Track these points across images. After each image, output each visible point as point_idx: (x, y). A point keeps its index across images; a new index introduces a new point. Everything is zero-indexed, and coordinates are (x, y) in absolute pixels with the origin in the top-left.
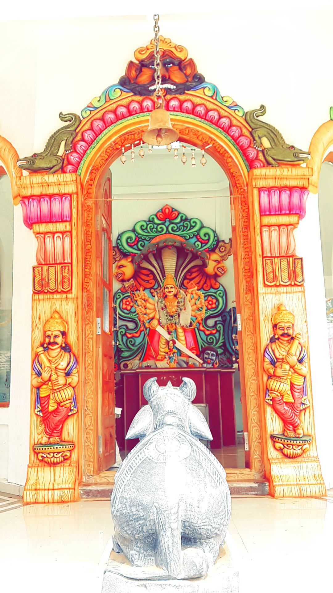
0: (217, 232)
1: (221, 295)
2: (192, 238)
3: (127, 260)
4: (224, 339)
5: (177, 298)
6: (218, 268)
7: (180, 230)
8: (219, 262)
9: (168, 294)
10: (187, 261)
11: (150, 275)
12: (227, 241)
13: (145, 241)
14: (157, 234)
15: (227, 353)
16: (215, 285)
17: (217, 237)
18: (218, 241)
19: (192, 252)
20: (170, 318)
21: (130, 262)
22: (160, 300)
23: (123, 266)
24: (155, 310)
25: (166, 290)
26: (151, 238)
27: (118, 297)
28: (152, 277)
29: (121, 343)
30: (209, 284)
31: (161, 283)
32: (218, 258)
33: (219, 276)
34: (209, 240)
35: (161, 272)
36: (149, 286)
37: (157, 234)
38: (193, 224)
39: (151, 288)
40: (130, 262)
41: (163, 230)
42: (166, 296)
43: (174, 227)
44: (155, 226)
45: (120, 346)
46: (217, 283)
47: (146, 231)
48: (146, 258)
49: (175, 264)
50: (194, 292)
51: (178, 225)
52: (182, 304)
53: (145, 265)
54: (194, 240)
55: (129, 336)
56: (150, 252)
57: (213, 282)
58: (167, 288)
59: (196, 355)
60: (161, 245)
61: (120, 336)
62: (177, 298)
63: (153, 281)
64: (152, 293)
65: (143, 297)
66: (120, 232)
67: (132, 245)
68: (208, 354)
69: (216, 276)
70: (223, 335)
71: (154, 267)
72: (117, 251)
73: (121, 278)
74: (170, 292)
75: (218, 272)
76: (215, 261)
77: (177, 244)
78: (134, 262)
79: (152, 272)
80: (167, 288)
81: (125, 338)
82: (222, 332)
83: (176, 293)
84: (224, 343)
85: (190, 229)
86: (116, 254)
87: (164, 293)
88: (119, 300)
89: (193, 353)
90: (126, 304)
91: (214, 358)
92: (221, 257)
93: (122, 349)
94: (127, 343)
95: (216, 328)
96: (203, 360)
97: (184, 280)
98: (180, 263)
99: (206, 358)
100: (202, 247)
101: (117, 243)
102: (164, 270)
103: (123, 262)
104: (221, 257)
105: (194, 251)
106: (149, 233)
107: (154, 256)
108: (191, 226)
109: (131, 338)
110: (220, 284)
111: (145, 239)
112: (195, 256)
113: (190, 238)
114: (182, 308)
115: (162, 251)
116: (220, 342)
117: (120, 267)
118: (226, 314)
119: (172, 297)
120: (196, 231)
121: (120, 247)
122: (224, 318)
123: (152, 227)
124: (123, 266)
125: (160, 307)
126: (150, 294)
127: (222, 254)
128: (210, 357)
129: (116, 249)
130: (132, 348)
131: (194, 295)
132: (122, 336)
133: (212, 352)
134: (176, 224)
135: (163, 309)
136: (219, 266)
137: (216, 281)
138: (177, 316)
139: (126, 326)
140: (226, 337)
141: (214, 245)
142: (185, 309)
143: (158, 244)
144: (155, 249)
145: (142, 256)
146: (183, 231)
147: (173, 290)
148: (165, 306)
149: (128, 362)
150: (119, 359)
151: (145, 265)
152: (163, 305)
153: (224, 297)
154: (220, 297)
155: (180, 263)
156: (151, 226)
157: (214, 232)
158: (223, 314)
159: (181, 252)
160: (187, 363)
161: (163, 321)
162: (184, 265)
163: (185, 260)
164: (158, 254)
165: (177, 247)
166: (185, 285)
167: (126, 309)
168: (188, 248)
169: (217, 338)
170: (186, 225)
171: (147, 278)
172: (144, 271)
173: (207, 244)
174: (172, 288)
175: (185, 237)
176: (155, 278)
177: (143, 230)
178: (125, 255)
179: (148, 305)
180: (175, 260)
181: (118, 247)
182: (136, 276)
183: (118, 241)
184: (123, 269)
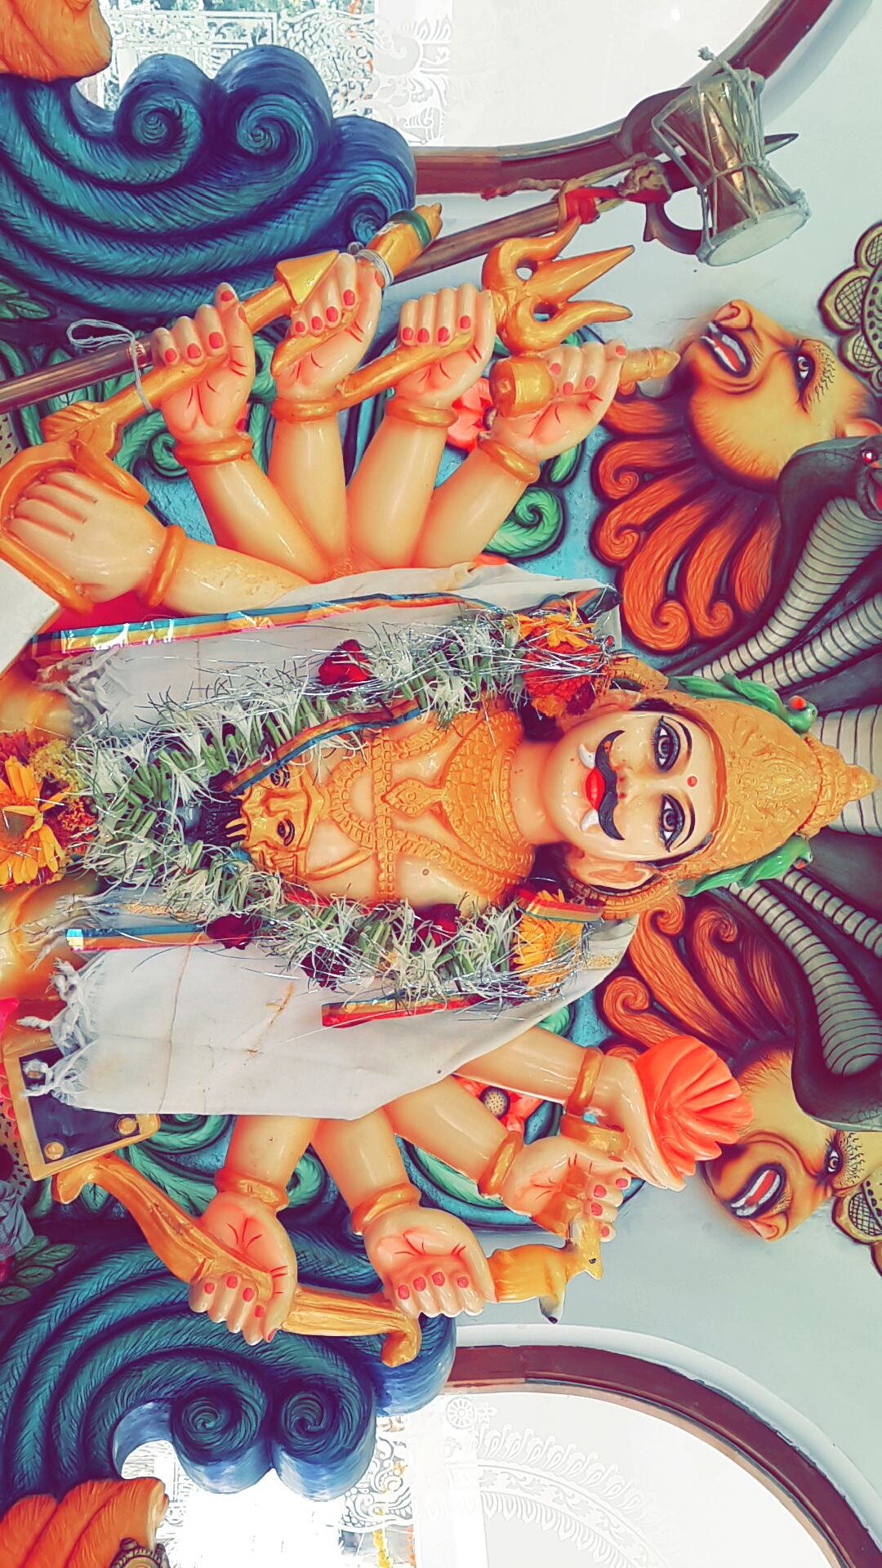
5: (515, 893)
6: (777, 1169)
9: (576, 758)
11: (724, 612)
20: (185, 785)
22: (478, 639)
24: (335, 562)
25: (635, 735)
28: (707, 628)
42: (539, 731)
52: (417, 968)
58: (667, 753)
62: (515, 893)
63: (673, 636)
65: (529, 385)
73: (706, 364)
74: (604, 788)
80: (667, 753)
83: (587, 872)
87: (582, 700)
114: (359, 985)
119: (532, 826)
125: (364, 627)
135: (339, 671)
138: (203, 897)
142: (333, 1016)
148: (386, 715)
152: (394, 668)
161: (135, 676)
171: (700, 583)
172: (757, 562)
174: (673, 815)
179: (412, 460)
184: (781, 381)
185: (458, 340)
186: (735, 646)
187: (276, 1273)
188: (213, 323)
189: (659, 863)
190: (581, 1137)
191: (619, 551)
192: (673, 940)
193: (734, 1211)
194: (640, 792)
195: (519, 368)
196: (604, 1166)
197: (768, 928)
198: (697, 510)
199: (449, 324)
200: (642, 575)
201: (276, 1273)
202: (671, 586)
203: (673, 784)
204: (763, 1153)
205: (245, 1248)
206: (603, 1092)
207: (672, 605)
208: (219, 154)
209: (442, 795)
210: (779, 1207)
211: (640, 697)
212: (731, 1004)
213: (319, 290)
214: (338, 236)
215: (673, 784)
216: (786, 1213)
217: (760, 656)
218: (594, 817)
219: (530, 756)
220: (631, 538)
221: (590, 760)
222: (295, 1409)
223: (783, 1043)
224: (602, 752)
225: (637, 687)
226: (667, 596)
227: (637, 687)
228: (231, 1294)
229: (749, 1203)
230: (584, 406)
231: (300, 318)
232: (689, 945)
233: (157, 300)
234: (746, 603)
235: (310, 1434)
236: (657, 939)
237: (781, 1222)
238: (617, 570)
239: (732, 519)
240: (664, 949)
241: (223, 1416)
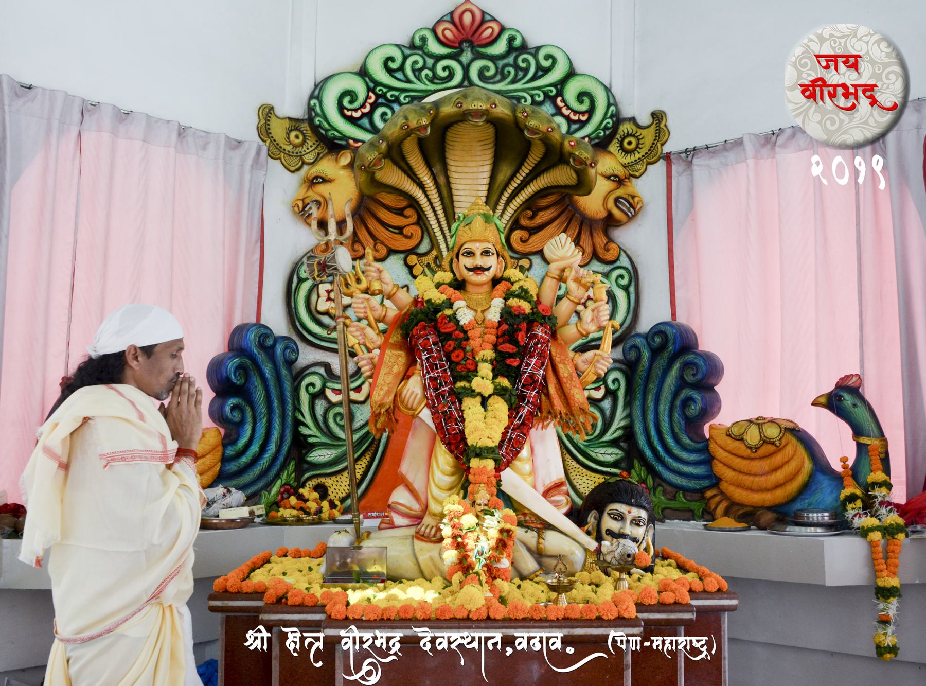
0: (613, 90)
1: (624, 282)
2: (541, 104)
3: (337, 160)
4: (629, 416)
6: (617, 200)
7: (504, 78)
8: (620, 181)
9: (472, 277)
10: (524, 171)
11: (408, 212)
12: (644, 119)
13: (396, 107)
14: (432, 87)
15: (636, 464)
16: (608, 250)
17: (616, 105)
18: (618, 120)
19: (546, 141)
21: (345, 167)
23: (325, 181)
25: (466, 261)
26: (413, 98)
27: (303, 275)
28: (414, 218)
29: (308, 420)
30: (589, 249)
31: (440, 238)
32: (620, 171)
33: (617, 224)
34: (591, 111)
35: (443, 203)
36: (403, 244)
37: (432, 87)
38: (546, 64)
39: (412, 251)
40: (345, 167)
41: (451, 76)
43: (487, 68)
44: (430, 62)
45: (304, 431)
46: (612, 245)
47: (399, 75)
48: (395, 154)
49: (487, 181)
50: (570, 275)
51: (501, 63)
53: (392, 176)
54: (548, 108)
55: (334, 398)
56: (408, 132)
57: (600, 240)
58: (470, 254)
59: (568, 514)
60: (448, 110)
61: (305, 398)
63: (416, 231)
64: (410, 268)
65: (376, 286)
66: (319, 79)
67: (357, 115)
68: (619, 517)
69: (610, 222)
70: (628, 404)
71: (421, 186)
72: (309, 133)
74: (478, 270)
75: (616, 212)
76: (608, 178)
77: (502, 110)
78: (357, 163)
79: (413, 203)
80: (470, 254)
81: (320, 406)
82: (621, 394)
84: (629, 433)
85: (534, 78)
86: (304, 141)
88: (306, 286)
89: (556, 504)
90: (329, 299)
91: (639, 532)
92: (625, 166)
93: (311, 440)
94: (327, 426)
95: (605, 383)
96: (599, 539)
97: (511, 230)
98: (502, 177)
99: (610, 532)
100: (570, 133)
101: (311, 109)
102: (451, 195)
103: (327, 167)
104: (624, 166)
105: (556, 136)
106: (408, 81)
107: (422, 144)
108: (539, 67)
109: (340, 404)
110: (620, 248)
111: (397, 100)
112: (555, 156)
113: (534, 103)
115: (450, 135)
116: (616, 425)
117: (314, 182)
118: (639, 341)
120: (554, 85)
121: (317, 121)
122: (633, 355)
123: (420, 65)
124: (325, 181)
126: (406, 270)
127: (628, 159)
128: (628, 529)
129: (305, 127)
130: (342, 435)
131: (572, 285)
132: (314, 397)
133: (636, 512)
134: (493, 58)
136: (620, 192)
137: (610, 240)
139: (327, 366)
140: (637, 413)
141: (605, 128)
143: (437, 105)
144: (425, 121)
145: (384, 146)
146: (514, 81)
147: (491, 261)
149: (328, 482)
150: (299, 471)
151: (392, 176)
153: (632, 289)
154: (619, 286)
155: (502, 177)
156: (415, 62)
157: (608, 90)
158: (630, 342)
159: (510, 141)
160: (538, 554)
162: (514, 184)
163: (517, 171)
164: (436, 144)
165: (496, 123)
166: (514, 245)
167: (327, 313)
168: (533, 123)
169: (608, 413)
170: (523, 65)
173: (583, 124)
174: (486, 253)
175: (518, 99)
176: (421, 221)
177: (390, 71)
178: (333, 145)
180: (488, 168)
181: (310, 120)
182: (363, 209)
183: (313, 102)
184: (323, 189)
185: (366, 304)
186: (422, 209)
187: (595, 355)
188: (364, 362)
189: (498, 255)
190: (567, 277)
191: (384, 251)
192: (531, 234)
193: (633, 216)
194: (479, 261)
195: (372, 289)
196: (573, 273)
197: (527, 200)
198: (370, 222)
199: (362, 306)
200: (393, 242)
201: (595, 355)
202: (397, 231)
203: (478, 253)
204: (611, 204)
205: (590, 362)
206: (557, 272)
207: (405, 231)
208: (243, 392)
209: (479, 310)
210: (630, 200)
211: (455, 260)
212: (555, 214)
213: (354, 336)
214: (271, 351)
215: (478, 253)
216: (633, 197)
217: (426, 199)
218: (486, 273)
219: (469, 288)
220: (379, 246)
221: (471, 273)
222: (689, 378)
223: (570, 196)
224: (469, 270)
225: (452, 260)
226: (401, 233)
227: (452, 260)
228: (599, 365)
229: (629, 211)
230: (380, 272)
231: (361, 342)
232: (533, 229)
233: (289, 421)
234: (404, 204)
235: (697, 372)
236: (531, 241)
237: (636, 199)
238: (391, 252)
239: (373, 208)
240: (534, 238)
241: (691, 403)
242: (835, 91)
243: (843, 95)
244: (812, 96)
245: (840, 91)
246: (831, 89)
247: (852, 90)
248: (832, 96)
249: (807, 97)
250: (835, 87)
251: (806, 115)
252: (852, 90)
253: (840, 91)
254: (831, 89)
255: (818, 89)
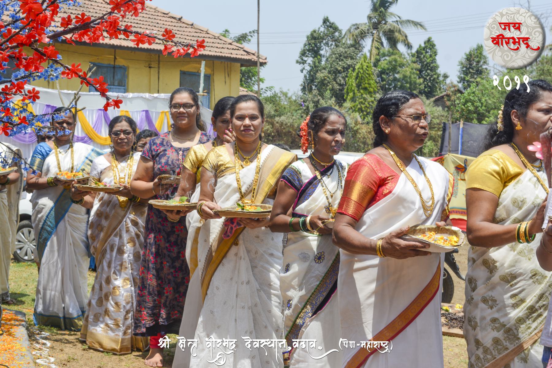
242: (509, 41)
243: (513, 42)
244: (497, 43)
245: (511, 41)
246: (507, 40)
247: (517, 40)
248: (507, 43)
249: (495, 44)
250: (509, 39)
251: (494, 52)
252: (517, 40)
253: (511, 41)
254: (507, 40)
255: (500, 40)
